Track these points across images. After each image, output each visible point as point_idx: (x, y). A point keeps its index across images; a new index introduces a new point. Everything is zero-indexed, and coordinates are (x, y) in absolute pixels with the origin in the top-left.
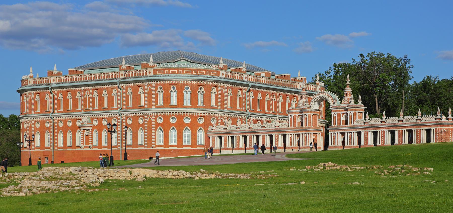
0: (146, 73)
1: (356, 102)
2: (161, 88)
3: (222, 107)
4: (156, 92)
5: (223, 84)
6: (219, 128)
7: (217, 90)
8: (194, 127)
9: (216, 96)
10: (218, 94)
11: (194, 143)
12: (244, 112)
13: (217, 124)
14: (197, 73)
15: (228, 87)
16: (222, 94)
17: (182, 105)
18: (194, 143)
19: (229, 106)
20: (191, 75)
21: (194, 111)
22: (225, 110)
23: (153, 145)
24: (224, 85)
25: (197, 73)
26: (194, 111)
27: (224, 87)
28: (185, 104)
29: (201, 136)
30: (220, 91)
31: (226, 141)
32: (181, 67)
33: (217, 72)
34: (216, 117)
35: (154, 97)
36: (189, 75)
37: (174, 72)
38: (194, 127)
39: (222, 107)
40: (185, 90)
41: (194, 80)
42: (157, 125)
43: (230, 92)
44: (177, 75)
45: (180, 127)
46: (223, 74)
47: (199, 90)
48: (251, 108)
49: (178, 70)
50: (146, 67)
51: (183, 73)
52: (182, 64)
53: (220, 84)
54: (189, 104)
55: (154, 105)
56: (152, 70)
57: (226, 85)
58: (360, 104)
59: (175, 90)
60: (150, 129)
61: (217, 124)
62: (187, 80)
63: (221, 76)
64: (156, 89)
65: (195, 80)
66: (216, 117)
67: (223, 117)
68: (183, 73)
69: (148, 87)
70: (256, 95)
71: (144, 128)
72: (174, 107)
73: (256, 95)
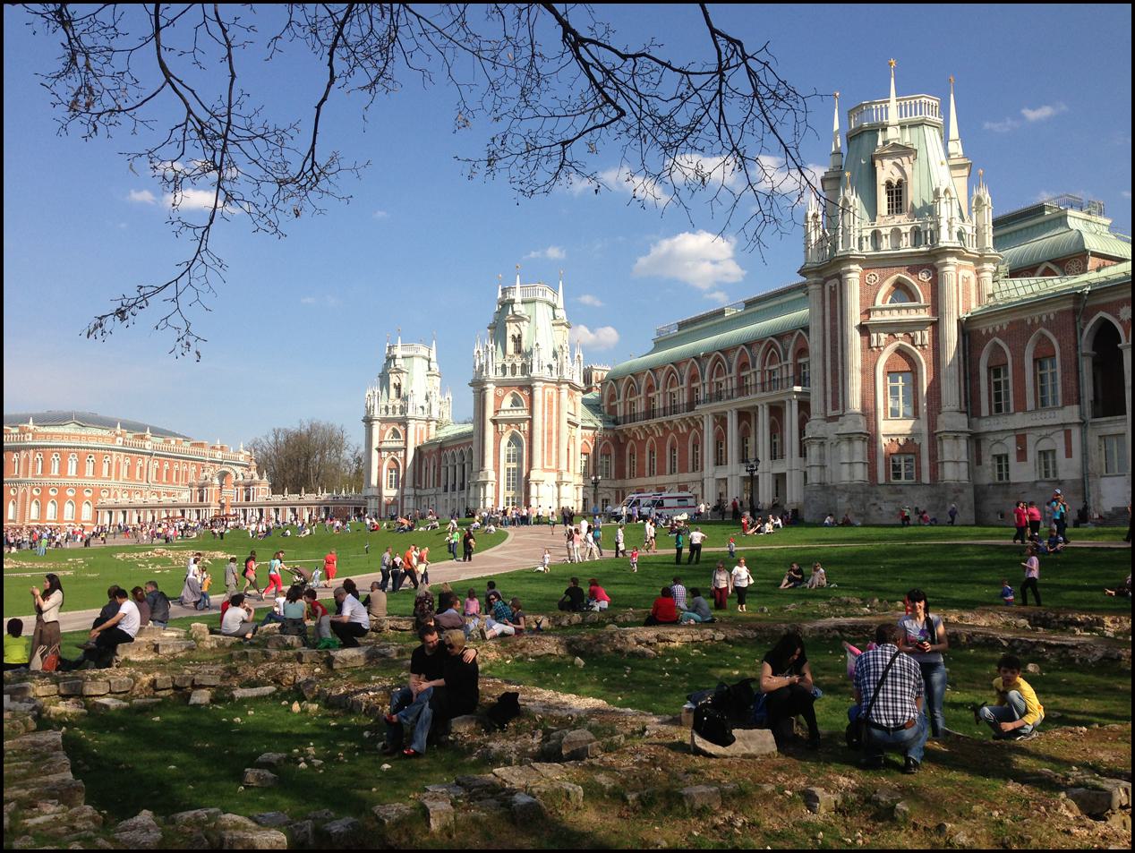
1: (261, 478)
3: (117, 477)
6: (110, 502)
8: (78, 501)
11: (77, 518)
12: (145, 483)
13: (109, 497)
16: (118, 464)
18: (77, 518)
19: (125, 475)
21: (79, 481)
22: (121, 481)
23: (27, 520)
26: (79, 481)
28: (69, 474)
29: (87, 512)
31: (116, 516)
32: (73, 431)
35: (31, 465)
38: (78, 501)
39: (117, 477)
41: (82, 447)
42: (33, 497)
43: (128, 461)
45: (61, 499)
48: (154, 479)
50: (23, 431)
52: (70, 429)
53: (114, 453)
54: (74, 474)
55: (30, 473)
56: (31, 435)
57: (123, 454)
58: (265, 479)
60: (24, 501)
61: (109, 497)
62: (74, 447)
63: (117, 443)
64: (34, 456)
65: (84, 448)
70: (161, 464)
73: (161, 464)
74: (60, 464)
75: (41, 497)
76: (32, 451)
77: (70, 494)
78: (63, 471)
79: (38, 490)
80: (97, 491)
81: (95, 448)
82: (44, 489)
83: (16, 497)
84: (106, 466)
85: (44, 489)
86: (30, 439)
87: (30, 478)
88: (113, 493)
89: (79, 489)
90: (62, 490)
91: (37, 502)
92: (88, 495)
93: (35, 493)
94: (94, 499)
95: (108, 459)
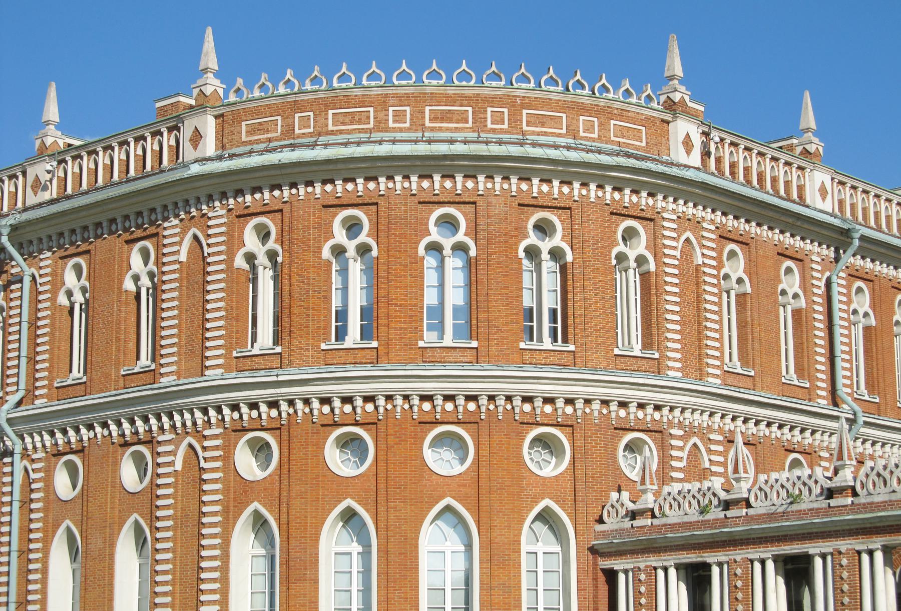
0: (176, 150)
2: (264, 236)
4: (230, 261)
5: (690, 210)
7: (655, 247)
9: (649, 285)
10: (660, 273)
12: (822, 403)
14: (515, 120)
15: (725, 237)
17: (412, 344)
20: (473, 136)
24: (700, 213)
25: (515, 120)
27: (696, 224)
30: (673, 249)
33: (648, 122)
34: (658, 432)
35: (216, 297)
36: (459, 136)
37: (353, 119)
39: (695, 363)
40: (435, 234)
42: (239, 492)
43: (737, 269)
44: (376, 136)
46: (688, 144)
47: (532, 239)
49: (382, 104)
51: (417, 124)
53: (670, 208)
55: (215, 353)
59: (363, 238)
62: (446, 166)
64: (234, 241)
66: (658, 432)
67: (703, 433)
68: (417, 124)
69: (182, 235)
71: (153, 519)
72: (353, 357)
74: (373, 272)
75: (279, 491)
76: (218, 213)
77: (442, 462)
78: (391, 318)
79: (261, 449)
80: (593, 438)
81: (566, 172)
82: (294, 440)
83: (148, 501)
84: (629, 287)
85: (294, 440)
86: (210, 147)
87: (214, 376)
88: (680, 457)
89: (493, 429)
90: (394, 433)
91: (259, 523)
92: (549, 468)
93: (247, 464)
94: (580, 490)
95: (640, 247)
